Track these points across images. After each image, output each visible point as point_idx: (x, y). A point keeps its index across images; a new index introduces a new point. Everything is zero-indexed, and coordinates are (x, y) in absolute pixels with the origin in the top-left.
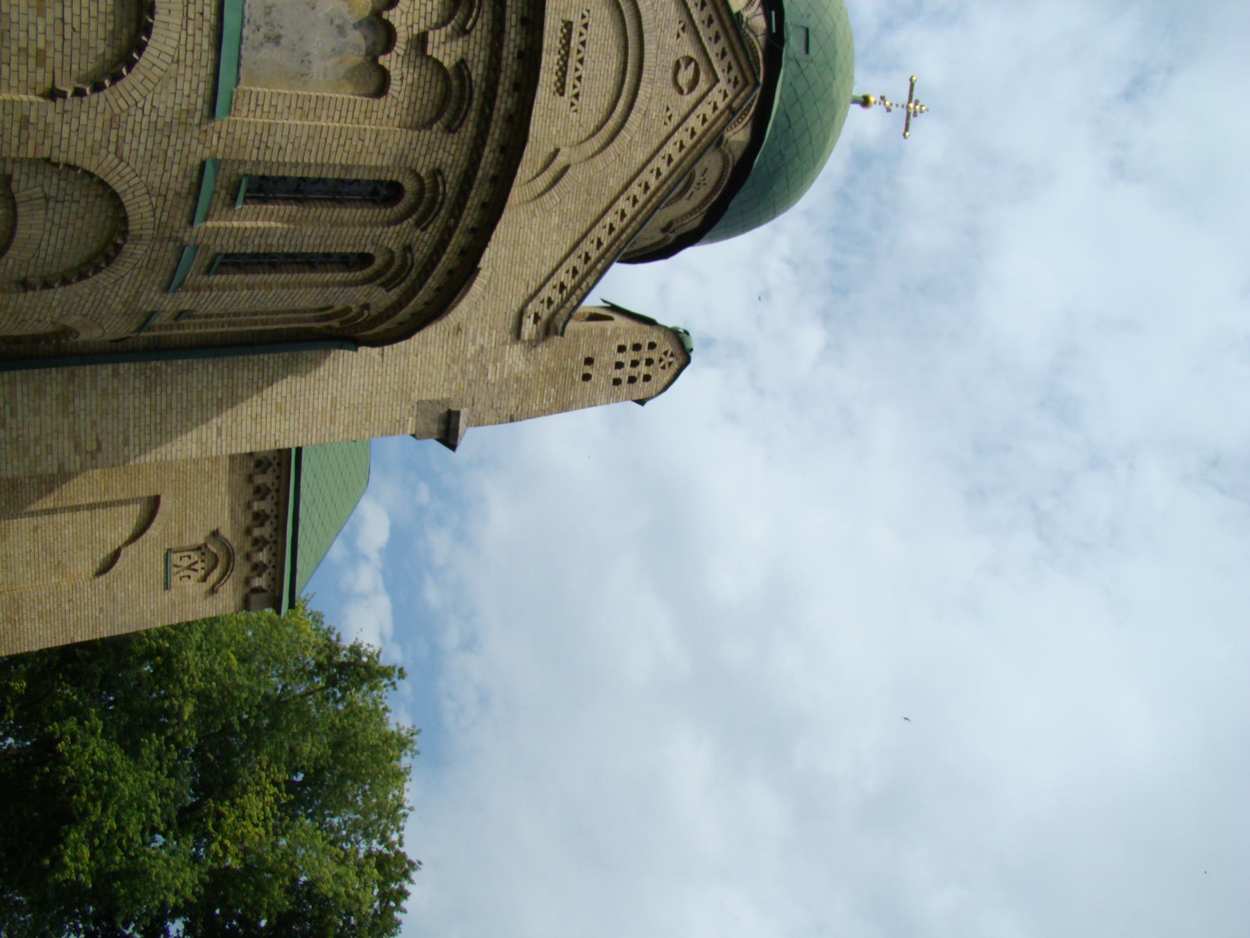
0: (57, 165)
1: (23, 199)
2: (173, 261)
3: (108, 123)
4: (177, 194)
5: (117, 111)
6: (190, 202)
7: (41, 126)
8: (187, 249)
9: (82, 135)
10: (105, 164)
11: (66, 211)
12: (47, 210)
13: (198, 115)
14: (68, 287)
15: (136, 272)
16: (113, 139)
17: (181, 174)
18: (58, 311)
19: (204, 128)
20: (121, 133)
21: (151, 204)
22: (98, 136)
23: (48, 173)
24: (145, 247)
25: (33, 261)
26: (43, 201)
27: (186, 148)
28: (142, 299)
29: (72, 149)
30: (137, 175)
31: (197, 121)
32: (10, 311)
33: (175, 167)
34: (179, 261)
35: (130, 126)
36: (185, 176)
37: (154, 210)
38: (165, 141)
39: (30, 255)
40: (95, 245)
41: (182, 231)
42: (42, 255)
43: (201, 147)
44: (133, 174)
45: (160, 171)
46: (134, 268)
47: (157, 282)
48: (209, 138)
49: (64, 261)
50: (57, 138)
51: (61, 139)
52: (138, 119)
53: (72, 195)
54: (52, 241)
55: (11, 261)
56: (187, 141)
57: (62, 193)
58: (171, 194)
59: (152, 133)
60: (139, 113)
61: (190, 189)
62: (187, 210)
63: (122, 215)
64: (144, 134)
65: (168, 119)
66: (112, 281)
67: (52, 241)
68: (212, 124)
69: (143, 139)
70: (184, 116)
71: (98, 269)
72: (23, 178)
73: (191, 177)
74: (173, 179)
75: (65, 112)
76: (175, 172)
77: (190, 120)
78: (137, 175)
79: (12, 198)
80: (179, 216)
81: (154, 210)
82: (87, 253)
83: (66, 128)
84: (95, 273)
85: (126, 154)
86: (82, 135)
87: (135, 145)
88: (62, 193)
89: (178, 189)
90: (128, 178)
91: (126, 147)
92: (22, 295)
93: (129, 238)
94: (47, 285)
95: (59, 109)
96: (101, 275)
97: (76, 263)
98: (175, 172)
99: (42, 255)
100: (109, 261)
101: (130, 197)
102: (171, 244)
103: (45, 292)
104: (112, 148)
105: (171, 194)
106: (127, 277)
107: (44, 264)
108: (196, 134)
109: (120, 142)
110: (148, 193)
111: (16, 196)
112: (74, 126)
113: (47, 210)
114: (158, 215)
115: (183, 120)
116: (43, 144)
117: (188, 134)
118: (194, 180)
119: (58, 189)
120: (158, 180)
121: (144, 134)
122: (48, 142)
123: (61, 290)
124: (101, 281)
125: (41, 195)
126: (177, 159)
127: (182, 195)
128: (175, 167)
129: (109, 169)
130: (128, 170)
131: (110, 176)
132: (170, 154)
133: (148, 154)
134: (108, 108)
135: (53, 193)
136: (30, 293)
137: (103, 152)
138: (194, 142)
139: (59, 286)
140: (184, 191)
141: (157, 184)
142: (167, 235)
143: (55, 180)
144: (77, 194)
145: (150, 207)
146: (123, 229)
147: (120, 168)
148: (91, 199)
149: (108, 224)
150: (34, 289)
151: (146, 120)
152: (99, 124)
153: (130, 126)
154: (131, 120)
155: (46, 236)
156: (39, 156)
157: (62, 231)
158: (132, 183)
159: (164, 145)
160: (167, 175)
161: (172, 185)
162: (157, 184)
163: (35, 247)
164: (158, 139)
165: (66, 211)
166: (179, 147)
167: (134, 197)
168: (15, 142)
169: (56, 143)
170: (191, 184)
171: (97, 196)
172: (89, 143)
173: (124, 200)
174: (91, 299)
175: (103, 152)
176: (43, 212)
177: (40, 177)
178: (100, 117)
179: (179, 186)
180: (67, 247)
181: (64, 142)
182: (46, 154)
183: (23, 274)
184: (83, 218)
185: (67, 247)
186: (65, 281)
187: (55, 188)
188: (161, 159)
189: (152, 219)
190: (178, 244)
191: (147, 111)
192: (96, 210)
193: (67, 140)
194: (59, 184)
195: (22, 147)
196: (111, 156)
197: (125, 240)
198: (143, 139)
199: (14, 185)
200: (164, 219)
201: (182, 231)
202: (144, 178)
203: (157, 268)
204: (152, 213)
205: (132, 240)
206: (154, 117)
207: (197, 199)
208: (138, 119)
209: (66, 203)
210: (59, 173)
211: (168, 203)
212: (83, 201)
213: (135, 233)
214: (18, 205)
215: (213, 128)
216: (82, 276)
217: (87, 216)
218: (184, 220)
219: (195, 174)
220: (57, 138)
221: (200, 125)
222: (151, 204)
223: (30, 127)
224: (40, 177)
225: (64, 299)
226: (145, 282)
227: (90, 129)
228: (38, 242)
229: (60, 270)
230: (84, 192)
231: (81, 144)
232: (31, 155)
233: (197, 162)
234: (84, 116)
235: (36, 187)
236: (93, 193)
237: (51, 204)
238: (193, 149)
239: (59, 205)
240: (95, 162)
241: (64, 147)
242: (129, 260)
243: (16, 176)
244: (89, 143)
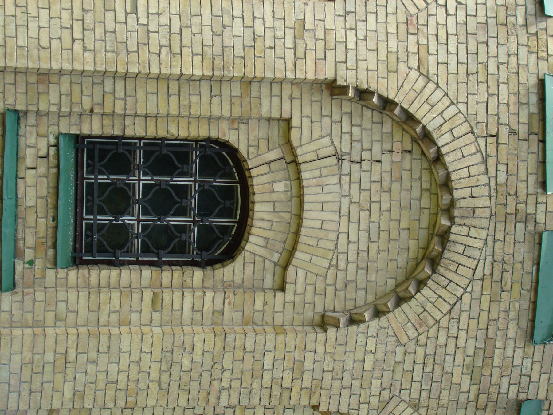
0: (344, 89)
1: (308, 157)
2: (529, 265)
3: (403, 27)
4: (513, 132)
5: (413, 10)
6: (535, 147)
7: (320, 34)
8: (545, 236)
9: (372, 46)
10: (407, 87)
11: (365, 177)
12: (340, 176)
13: (521, 11)
14: (383, 319)
15: (477, 286)
16: (413, 48)
17: (513, 99)
18: (376, 384)
19: (532, 30)
20: (423, 41)
21: (479, 151)
22: (393, 44)
23: (336, 117)
24: (483, 234)
25: (330, 281)
26: (334, 160)
27: (513, 60)
28: (497, 361)
29: (362, 65)
30: (452, 103)
31: (521, 20)
32: (307, 377)
33: (503, 88)
34: (538, 264)
35: (432, 30)
36: (520, 104)
37: (485, 161)
38: (482, 48)
39: (327, 265)
40: (413, 244)
41: (531, 199)
42: (342, 265)
43: (533, 57)
44: (446, 102)
45: (483, 97)
46: (472, 280)
47: (513, 315)
48: (542, 43)
49: (372, 277)
50: (341, 49)
51: (347, 50)
52: (442, 20)
53: (371, 150)
54: (353, 238)
55: (301, 273)
56: (513, 50)
57: (357, 146)
58: (504, 133)
59: (462, 39)
60: (442, 11)
61: (529, 124)
62: (533, 160)
63: (442, 173)
64: (452, 40)
65: (482, 20)
66: (446, 308)
67: (353, 238)
68: (542, 25)
69: (453, 50)
70: (502, 13)
71: (421, 284)
72: (306, 122)
73: (528, 104)
74: (503, 108)
75: (348, 13)
76: (503, 98)
77: (511, 19)
78: (452, 103)
79: (295, 162)
80: (523, 174)
81: (485, 161)
82: (402, 261)
83: (351, 35)
84: (418, 291)
85: (432, 70)
86: (372, 46)
87: (442, 58)
88: (357, 146)
89: (515, 127)
90: (440, 107)
91: (432, 60)
92: (321, 336)
93: (456, 213)
94: (353, 321)
95: (340, 12)
96: (425, 291)
97: (391, 283)
98: (503, 98)
99: (342, 265)
100: (434, 263)
101: (447, 138)
102: (520, 226)
103: (353, 329)
104: (413, 62)
105: (504, 133)
106: (466, 299)
107: (346, 282)
108: (523, 39)
109: (423, 50)
110: (472, 132)
111: (299, 151)
112: (361, 34)
113: (340, 176)
114: (492, 172)
115: (502, 19)
116: (325, 58)
117: (512, 39)
118: (534, 109)
119: (352, 141)
120: (482, 109)
121: (452, 40)
122: (330, 55)
123: (374, 323)
124: (429, 306)
125: (331, 150)
126: (503, 79)
127: (522, 136)
128: (503, 88)
129: (413, 94)
130: (439, 94)
131: (416, 105)
132: (492, 69)
133: (462, 69)
134: (401, 7)
135: (346, 150)
136: (332, 331)
137: (402, 67)
138: (523, 51)
139: (371, 319)
140: (523, 128)
141: (481, 118)
142: (511, 209)
143: (346, 128)
144: (377, 148)
145: (478, 158)
146: (446, 199)
147: (427, 92)
148: (397, 157)
149: (425, 202)
150: (337, 326)
151: (451, 19)
152: (392, 29)
153: (432, 30)
154: (432, 21)
155: (343, 228)
156: (321, 77)
157: (364, 214)
158: (448, 114)
159: (482, 57)
160: (493, 102)
161: (504, 119)
162: (481, 118)
163: (332, 246)
164: (472, 48)
165: (365, 177)
166: (503, 58)
167: (455, 139)
168: (290, 55)
169: (341, 58)
170: (530, 115)
171: (403, 151)
172: (383, 56)
173: (440, 143)
174: (420, 351)
175: (402, 67)
176: (335, 179)
177: (326, 120)
178: (391, 18)
179: (514, 119)
180: (374, 247)
181: (351, 55)
182: (330, 75)
183: (319, 309)
184: (390, 191)
185: (374, 247)
186: (378, 313)
187: (346, 137)
188: (482, 78)
189: (484, 179)
190: (530, 227)
191: (451, 10)
192: (405, 175)
193: (354, 52)
194: (351, 133)
195: (299, 63)
196: (414, 74)
197: (452, 219)
198: (453, 50)
199: (295, 134)
200: (502, 178)
201: (531, 199)
202: (462, 107)
203: (507, 276)
204: (482, 168)
205: (461, 217)
206: (461, 18)
207: (543, 141)
208: (442, 20)
209: (365, 165)
210: (351, 115)
211: (503, 148)
212: (387, 166)
213: (463, 203)
214: (303, 167)
215: (546, 30)
216: (400, 301)
217: (396, 186)
218: (532, 179)
219: (534, 99)
220: (341, 49)
221: (526, 25)
222: (479, 151)
223: (307, 34)
224: (326, 120)
225: (380, 355)
226: (494, 315)
227: (382, 37)
228: (333, 236)
229: (370, 299)
230: (387, 146)
231: (372, 56)
232: (311, 76)
233: (533, 81)
234: (371, 19)
235: (322, 137)
236: (397, 147)
237: (346, 165)
238: (523, 62)
239: (356, 167)
240: (393, 86)
241: (351, 63)
242: (462, 260)
243: (295, 122)
244: (383, 56)
